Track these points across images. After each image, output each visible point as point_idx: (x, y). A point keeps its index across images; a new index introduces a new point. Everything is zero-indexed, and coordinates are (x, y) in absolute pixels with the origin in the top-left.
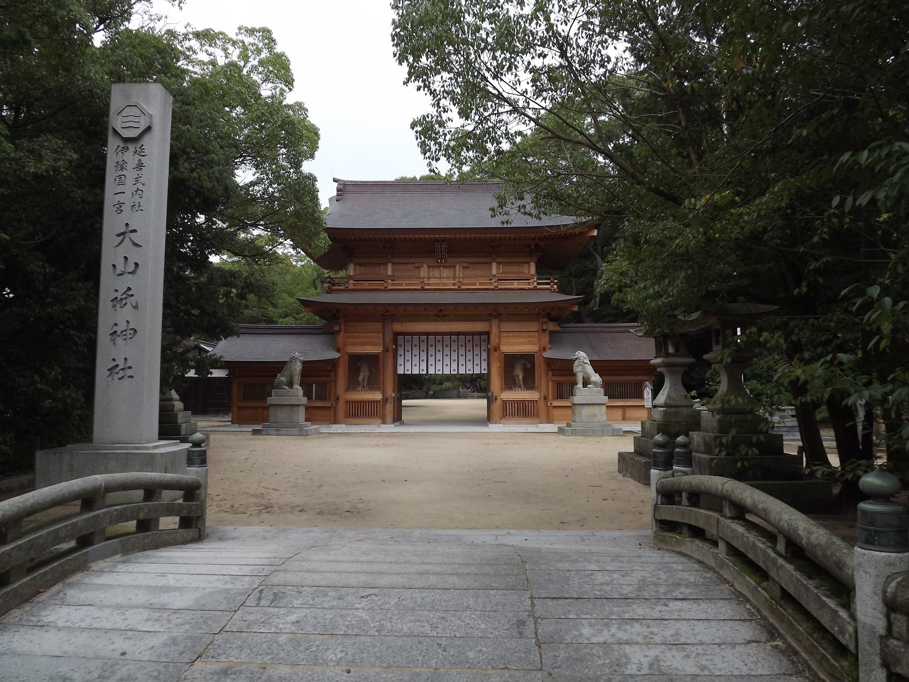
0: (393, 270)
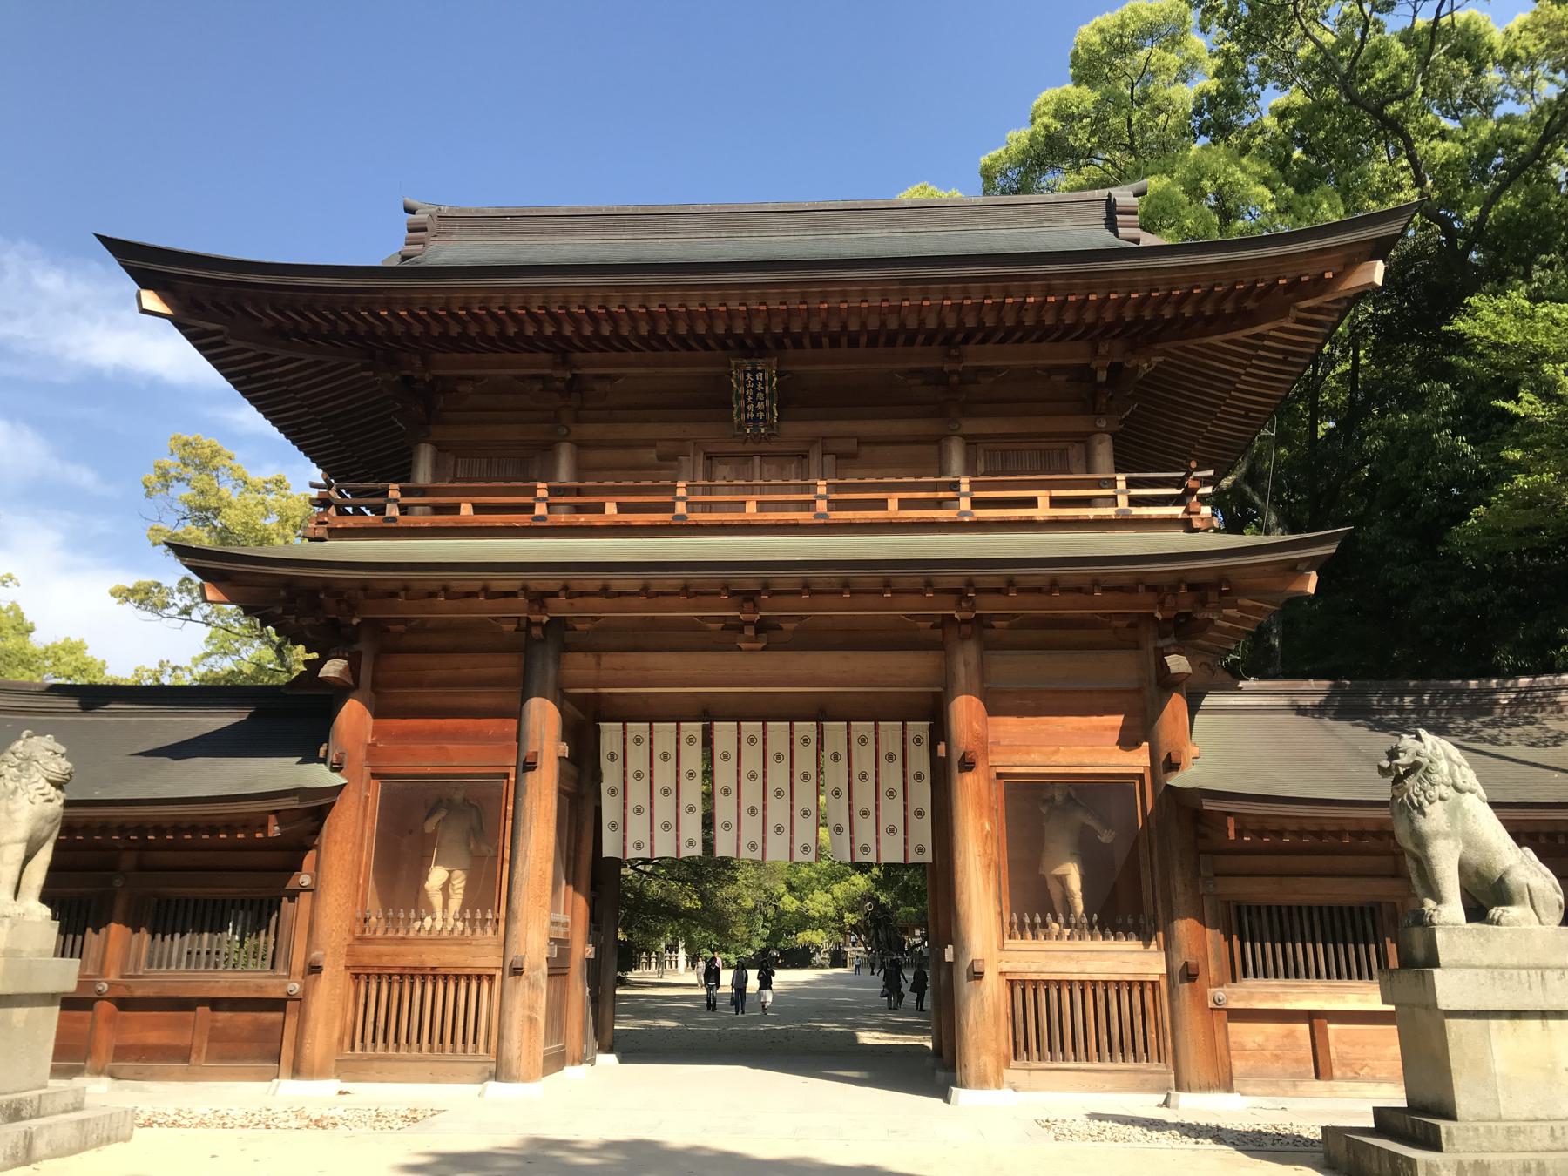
0: (580, 470)
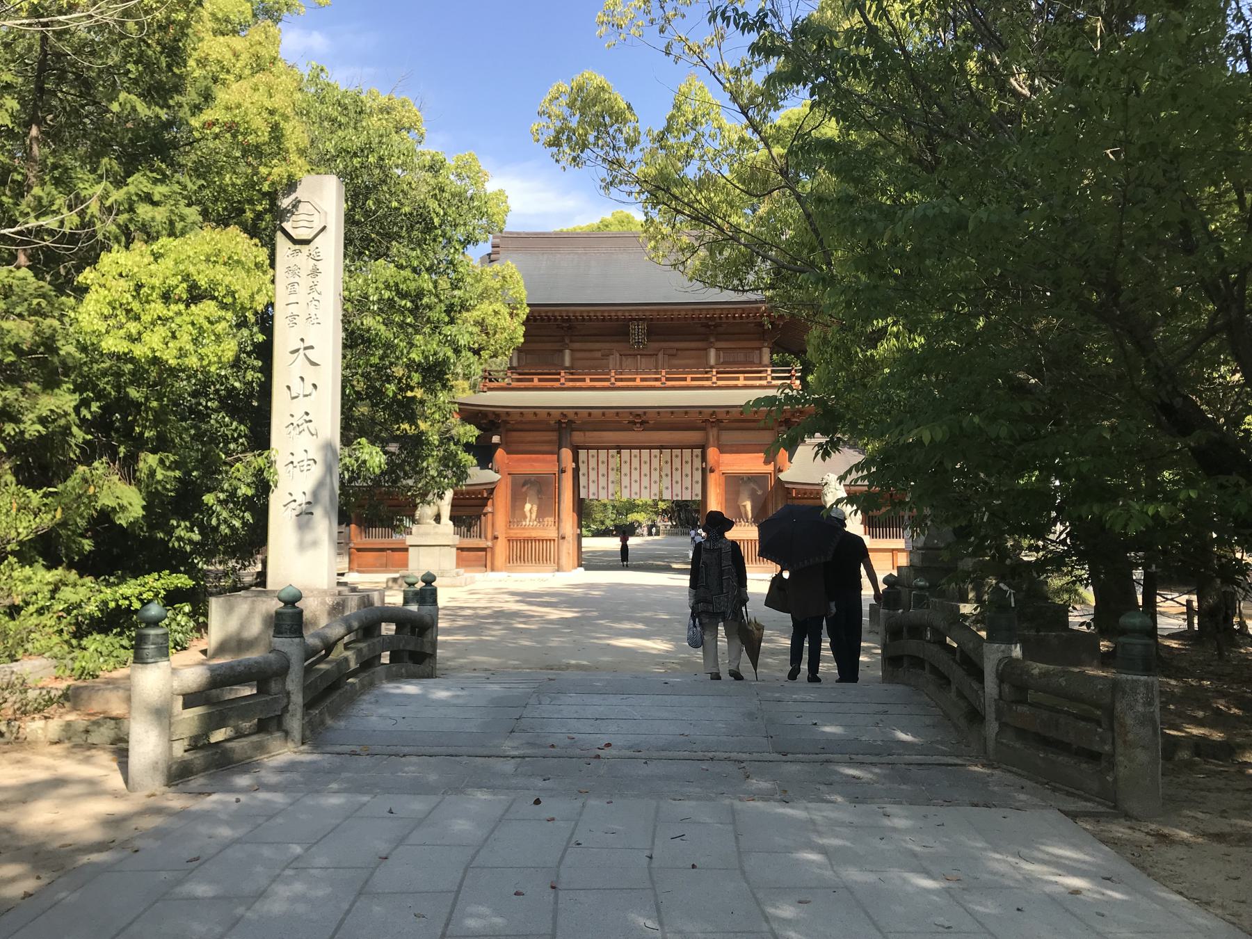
0: (573, 359)
